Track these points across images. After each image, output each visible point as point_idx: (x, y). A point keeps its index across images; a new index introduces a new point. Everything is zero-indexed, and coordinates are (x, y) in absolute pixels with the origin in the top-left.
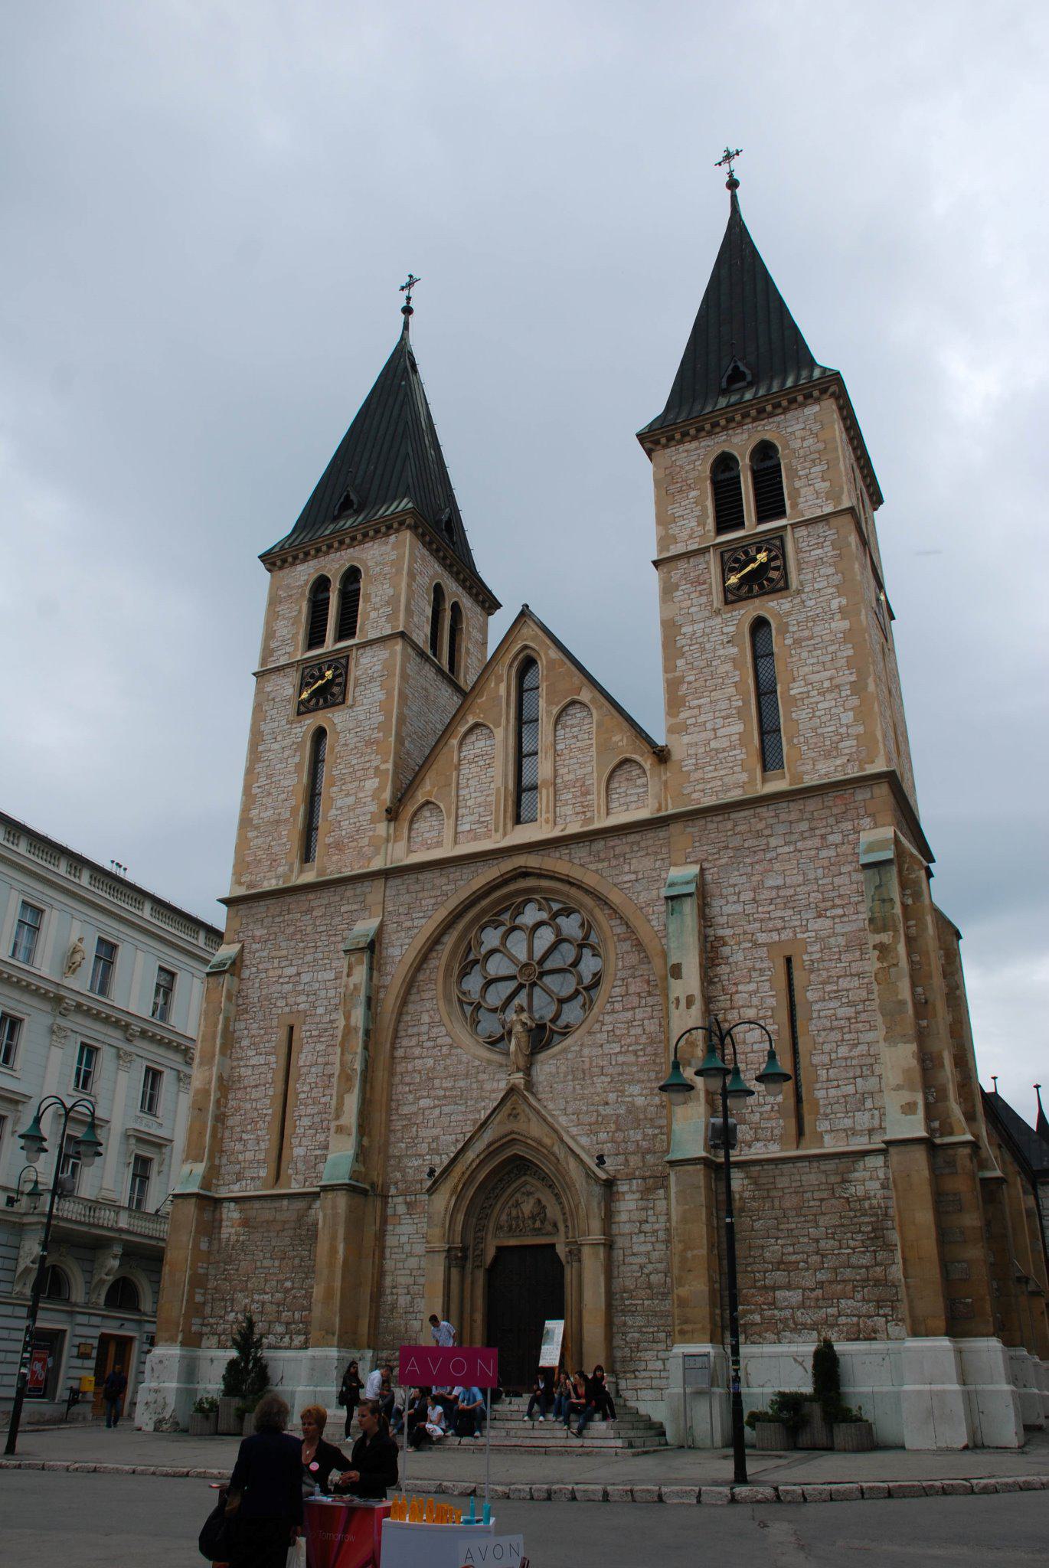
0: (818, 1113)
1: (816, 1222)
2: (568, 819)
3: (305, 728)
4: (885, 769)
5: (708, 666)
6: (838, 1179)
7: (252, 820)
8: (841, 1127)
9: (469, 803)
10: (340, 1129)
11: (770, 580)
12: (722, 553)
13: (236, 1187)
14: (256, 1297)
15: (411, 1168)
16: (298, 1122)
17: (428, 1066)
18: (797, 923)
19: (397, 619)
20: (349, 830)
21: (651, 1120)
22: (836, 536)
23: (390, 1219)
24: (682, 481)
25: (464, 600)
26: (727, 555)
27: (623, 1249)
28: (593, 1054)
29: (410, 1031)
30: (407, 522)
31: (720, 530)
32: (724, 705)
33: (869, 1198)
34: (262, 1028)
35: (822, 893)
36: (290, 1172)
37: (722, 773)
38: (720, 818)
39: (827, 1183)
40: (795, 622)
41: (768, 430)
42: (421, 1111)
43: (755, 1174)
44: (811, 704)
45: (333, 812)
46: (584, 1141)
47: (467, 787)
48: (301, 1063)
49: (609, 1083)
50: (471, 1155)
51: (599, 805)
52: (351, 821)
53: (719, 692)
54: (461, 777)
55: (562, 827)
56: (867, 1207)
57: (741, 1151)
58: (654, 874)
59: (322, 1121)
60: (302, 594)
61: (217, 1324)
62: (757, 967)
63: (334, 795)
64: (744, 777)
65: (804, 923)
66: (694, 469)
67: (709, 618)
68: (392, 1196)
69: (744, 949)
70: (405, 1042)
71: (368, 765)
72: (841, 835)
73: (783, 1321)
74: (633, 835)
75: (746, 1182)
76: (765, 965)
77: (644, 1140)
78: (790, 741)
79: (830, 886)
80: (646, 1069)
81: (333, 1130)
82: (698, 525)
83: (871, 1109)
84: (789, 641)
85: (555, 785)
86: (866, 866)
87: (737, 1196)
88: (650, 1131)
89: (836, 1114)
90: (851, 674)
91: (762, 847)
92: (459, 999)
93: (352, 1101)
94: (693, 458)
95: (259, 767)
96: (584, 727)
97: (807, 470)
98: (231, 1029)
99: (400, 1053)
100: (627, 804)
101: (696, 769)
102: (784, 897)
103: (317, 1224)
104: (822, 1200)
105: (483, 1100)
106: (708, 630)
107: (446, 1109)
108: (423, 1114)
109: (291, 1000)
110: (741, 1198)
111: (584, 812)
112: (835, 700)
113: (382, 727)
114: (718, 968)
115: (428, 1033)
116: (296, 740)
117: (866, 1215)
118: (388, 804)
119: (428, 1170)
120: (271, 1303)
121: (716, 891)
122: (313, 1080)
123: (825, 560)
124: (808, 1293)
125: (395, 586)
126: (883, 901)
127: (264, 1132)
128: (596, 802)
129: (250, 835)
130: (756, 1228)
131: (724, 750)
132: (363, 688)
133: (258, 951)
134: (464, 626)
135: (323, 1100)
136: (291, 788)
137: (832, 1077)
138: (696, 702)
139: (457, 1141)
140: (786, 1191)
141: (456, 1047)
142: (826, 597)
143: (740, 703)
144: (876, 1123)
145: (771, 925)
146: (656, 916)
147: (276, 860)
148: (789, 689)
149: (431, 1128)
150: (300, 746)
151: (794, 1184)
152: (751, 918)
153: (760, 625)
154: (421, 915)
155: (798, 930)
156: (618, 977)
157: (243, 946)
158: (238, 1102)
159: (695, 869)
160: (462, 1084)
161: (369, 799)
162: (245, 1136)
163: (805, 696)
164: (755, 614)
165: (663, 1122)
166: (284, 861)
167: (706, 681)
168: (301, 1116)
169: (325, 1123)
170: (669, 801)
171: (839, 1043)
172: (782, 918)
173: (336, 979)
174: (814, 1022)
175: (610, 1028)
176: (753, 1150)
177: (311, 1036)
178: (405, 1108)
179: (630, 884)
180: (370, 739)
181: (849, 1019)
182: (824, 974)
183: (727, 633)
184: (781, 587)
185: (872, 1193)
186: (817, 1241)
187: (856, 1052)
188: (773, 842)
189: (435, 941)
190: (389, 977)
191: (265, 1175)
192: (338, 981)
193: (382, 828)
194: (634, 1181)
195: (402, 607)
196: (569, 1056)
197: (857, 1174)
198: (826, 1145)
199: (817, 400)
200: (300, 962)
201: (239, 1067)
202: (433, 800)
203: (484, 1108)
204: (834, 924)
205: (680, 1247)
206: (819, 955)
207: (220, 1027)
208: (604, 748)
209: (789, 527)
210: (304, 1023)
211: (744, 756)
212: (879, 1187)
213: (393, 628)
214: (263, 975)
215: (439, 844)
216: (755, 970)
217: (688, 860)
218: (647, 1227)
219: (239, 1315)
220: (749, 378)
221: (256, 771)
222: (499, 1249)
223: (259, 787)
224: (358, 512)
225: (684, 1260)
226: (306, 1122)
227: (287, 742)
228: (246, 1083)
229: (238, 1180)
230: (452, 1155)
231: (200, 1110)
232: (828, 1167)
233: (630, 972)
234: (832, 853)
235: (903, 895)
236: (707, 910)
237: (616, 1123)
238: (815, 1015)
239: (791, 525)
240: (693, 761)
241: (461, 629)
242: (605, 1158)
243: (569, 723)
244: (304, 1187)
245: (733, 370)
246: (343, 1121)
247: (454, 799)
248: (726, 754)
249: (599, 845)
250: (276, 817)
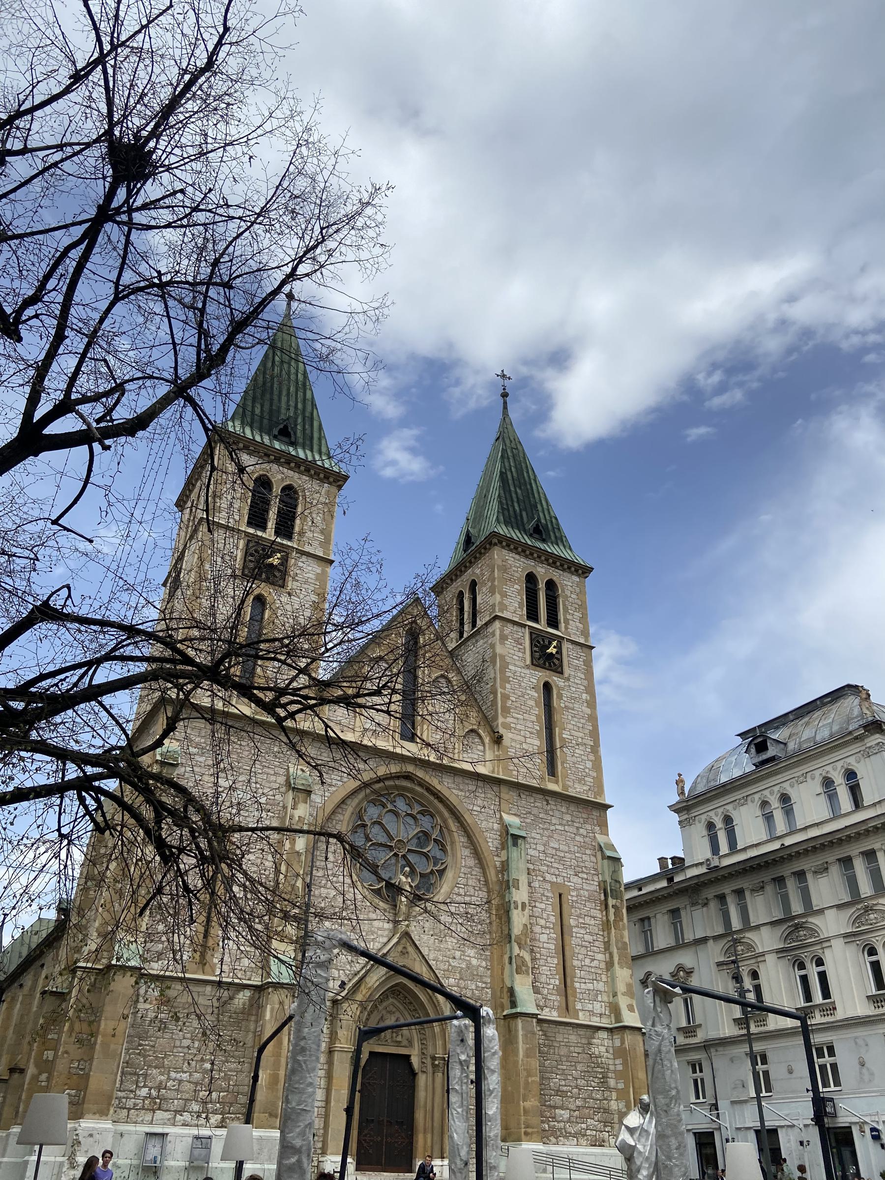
1: (575, 1066)
12: (531, 634)
14: (173, 1075)
18: (565, 875)
26: (534, 636)
30: (340, 483)
38: (527, 793)
41: (556, 575)
43: (545, 1029)
61: (127, 1098)
73: (560, 1129)
76: (550, 895)
78: (563, 763)
86: (609, 858)
104: (579, 1053)
120: (189, 1082)
124: (572, 1113)
138: (515, 715)
145: (552, 870)
153: (547, 687)
184: (559, 670)
186: (576, 1079)
189: (343, 802)
197: (595, 1041)
199: (579, 576)
213: (324, 553)
219: (152, 1091)
222: (371, 1053)
225: (527, 1083)
232: (581, 1033)
249: (459, 779)
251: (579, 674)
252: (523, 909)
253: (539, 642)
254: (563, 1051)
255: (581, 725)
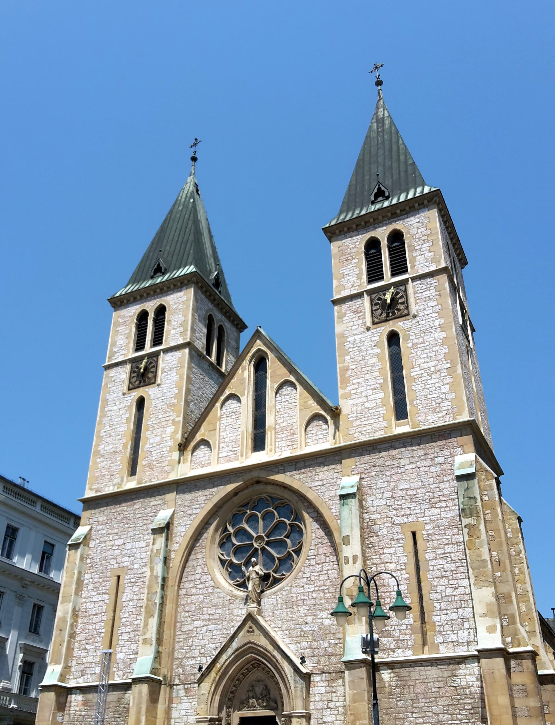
0: (435, 631)
1: (436, 702)
2: (283, 449)
3: (132, 397)
4: (468, 419)
5: (363, 360)
6: (450, 675)
7: (100, 451)
8: (450, 640)
9: (226, 440)
10: (145, 641)
11: (399, 310)
13: (81, 680)
15: (188, 665)
16: (120, 637)
17: (200, 600)
18: (419, 511)
19: (186, 335)
20: (156, 457)
21: (333, 634)
22: (437, 284)
23: (175, 700)
24: (349, 254)
25: (226, 324)
27: (317, 719)
28: (298, 592)
29: (190, 578)
31: (370, 281)
32: (372, 382)
33: (469, 687)
34: (101, 578)
35: (433, 493)
36: (115, 669)
37: (372, 421)
39: (442, 677)
40: (413, 334)
42: (195, 629)
44: (423, 381)
45: (148, 446)
46: (293, 647)
47: (225, 430)
48: (124, 600)
49: (308, 610)
50: (224, 657)
51: (301, 441)
52: (158, 451)
53: (369, 375)
54: (222, 425)
55: (280, 453)
56: (468, 693)
57: (389, 655)
58: (333, 481)
59: (135, 636)
60: (133, 321)
62: (395, 538)
63: (149, 436)
64: (385, 424)
65: (423, 511)
66: (355, 247)
67: (363, 332)
68: (176, 685)
69: (387, 527)
70: (186, 585)
71: (168, 418)
72: (443, 458)
74: (321, 459)
75: (392, 675)
76: (400, 536)
77: (329, 647)
79: (438, 489)
80: (330, 601)
81: (141, 642)
82: (358, 279)
83: (468, 629)
84: (410, 345)
85: (275, 429)
87: (387, 685)
88: (333, 641)
89: (446, 631)
90: (447, 363)
91: (396, 465)
92: (219, 557)
93: (154, 622)
94: (355, 241)
95: (105, 420)
96: (292, 396)
97: (421, 246)
98: (82, 579)
99: (182, 592)
100: (317, 440)
101: (357, 420)
102: (410, 495)
103: (129, 704)
105: (232, 622)
106: (363, 339)
107: (210, 627)
108: (196, 630)
109: (119, 560)
110: (389, 686)
111: (293, 445)
112: (438, 378)
113: (177, 396)
114: (372, 539)
115: (200, 579)
116: (127, 404)
117: (467, 698)
118: (179, 441)
119: (198, 667)
121: (370, 491)
122: (131, 610)
123: (431, 297)
125: (185, 316)
126: (470, 498)
127: (100, 644)
128: (299, 439)
129: (98, 460)
130: (399, 706)
131: (373, 408)
132: (166, 374)
133: (100, 530)
134: (226, 338)
135: (136, 623)
136: (123, 432)
137: (442, 608)
138: (355, 381)
139: (217, 648)
140: (417, 681)
141: (217, 588)
142: (432, 319)
143: (382, 381)
144: (472, 638)
146: (335, 506)
147: (113, 475)
148: (410, 373)
149: (201, 640)
150: (129, 407)
151: (422, 677)
152: (391, 508)
154: (198, 506)
155: (419, 515)
156: (313, 542)
157: (92, 527)
158: (84, 625)
159: (356, 478)
160: (219, 611)
161: (169, 438)
162: (88, 647)
163: (420, 376)
164: (390, 329)
165: (341, 636)
166: (118, 475)
167: (362, 368)
168: (122, 633)
169: (137, 637)
170: (341, 438)
171: (447, 586)
172: (409, 508)
173: (146, 547)
174: (431, 572)
175: (308, 575)
176: (395, 654)
177: (131, 582)
178: (186, 626)
179: (318, 487)
180: (170, 404)
181: (452, 571)
182: (436, 543)
183: (374, 341)
185: (471, 684)
186: (438, 715)
187: (456, 592)
188: (403, 462)
190: (178, 545)
191: (99, 672)
192: (148, 548)
193: (176, 455)
194: (324, 675)
195: (189, 328)
196: (284, 593)
197: (461, 671)
198: (441, 652)
200: (125, 536)
201: (86, 602)
202: (205, 438)
203: (233, 626)
204: (441, 512)
205: (352, 718)
206: (432, 531)
207: (75, 577)
208: (304, 407)
209: (410, 280)
210: (126, 574)
211: (384, 412)
212: (475, 680)
214: (103, 545)
215: (209, 464)
216: (394, 540)
217: (353, 473)
218: (331, 705)
220: (387, 194)
221: (103, 422)
223: (105, 432)
224: (164, 274)
226: (125, 637)
227: (122, 405)
228: (90, 613)
229: (82, 675)
230: (213, 657)
231: (61, 630)
233: (319, 540)
234: (438, 469)
235: (481, 495)
236: (364, 503)
237: (312, 636)
238: (431, 568)
239: (411, 278)
240: (355, 415)
241: (224, 340)
242: (306, 659)
243: (284, 393)
244: (122, 679)
245: (378, 189)
246: (147, 636)
247: (218, 438)
248: (374, 411)
250: (114, 450)
251: (429, 304)
252: (354, 562)
253: (379, 299)
254: (420, 689)
255: (435, 353)
